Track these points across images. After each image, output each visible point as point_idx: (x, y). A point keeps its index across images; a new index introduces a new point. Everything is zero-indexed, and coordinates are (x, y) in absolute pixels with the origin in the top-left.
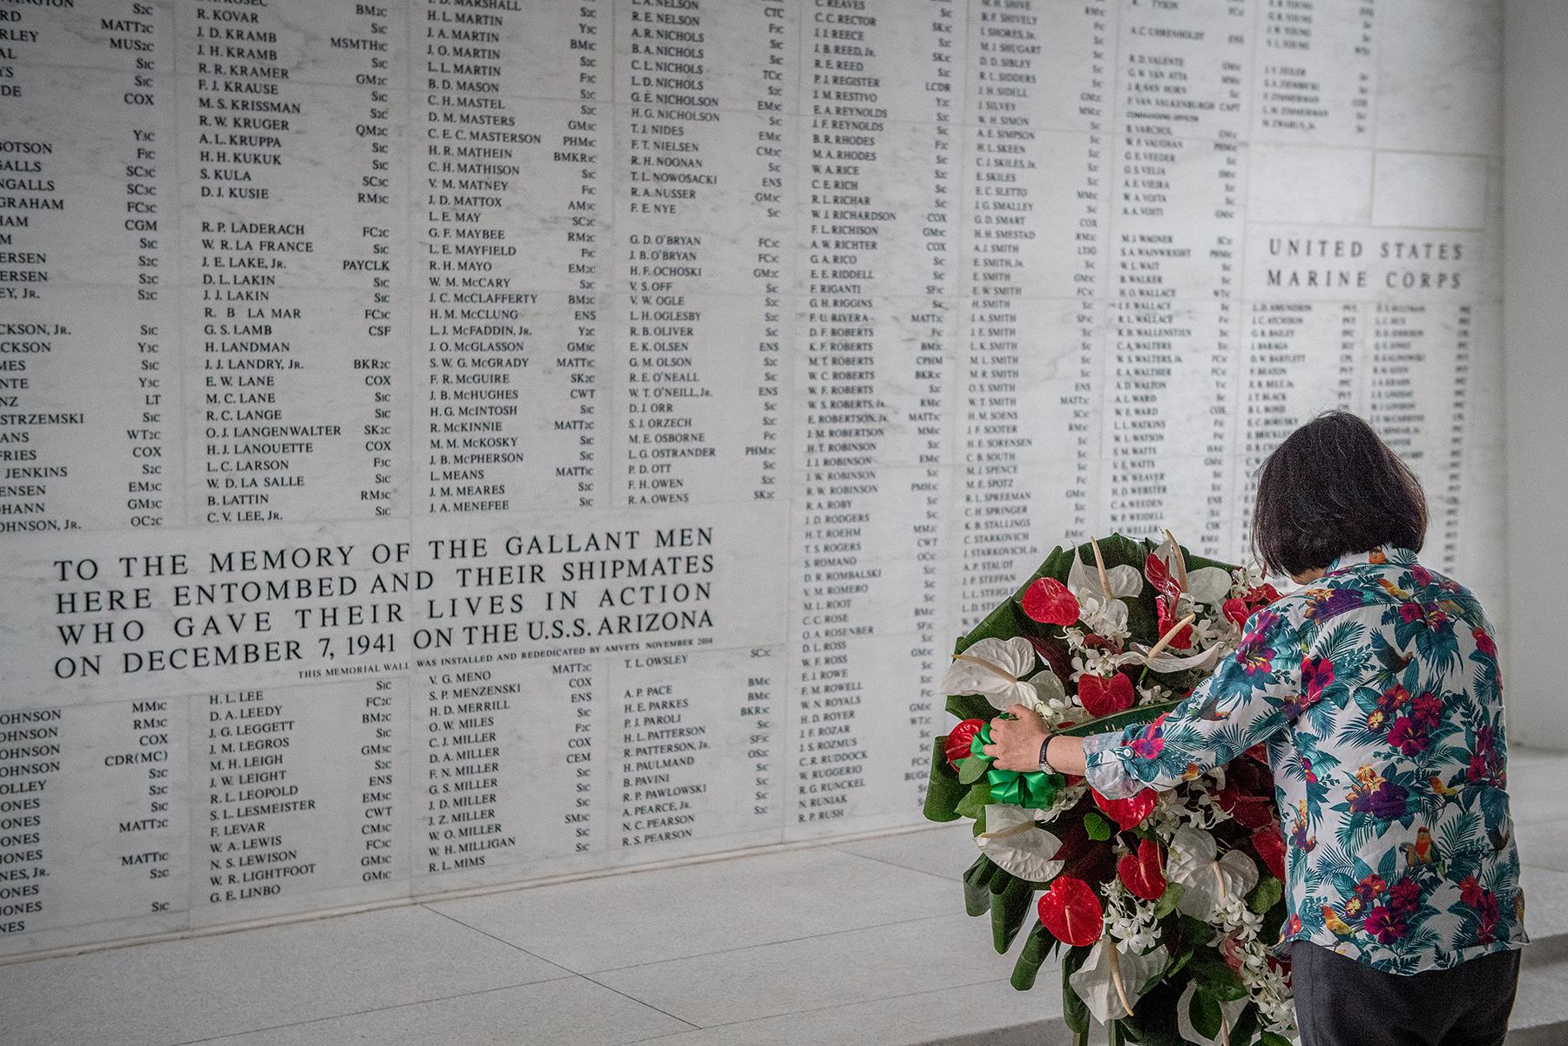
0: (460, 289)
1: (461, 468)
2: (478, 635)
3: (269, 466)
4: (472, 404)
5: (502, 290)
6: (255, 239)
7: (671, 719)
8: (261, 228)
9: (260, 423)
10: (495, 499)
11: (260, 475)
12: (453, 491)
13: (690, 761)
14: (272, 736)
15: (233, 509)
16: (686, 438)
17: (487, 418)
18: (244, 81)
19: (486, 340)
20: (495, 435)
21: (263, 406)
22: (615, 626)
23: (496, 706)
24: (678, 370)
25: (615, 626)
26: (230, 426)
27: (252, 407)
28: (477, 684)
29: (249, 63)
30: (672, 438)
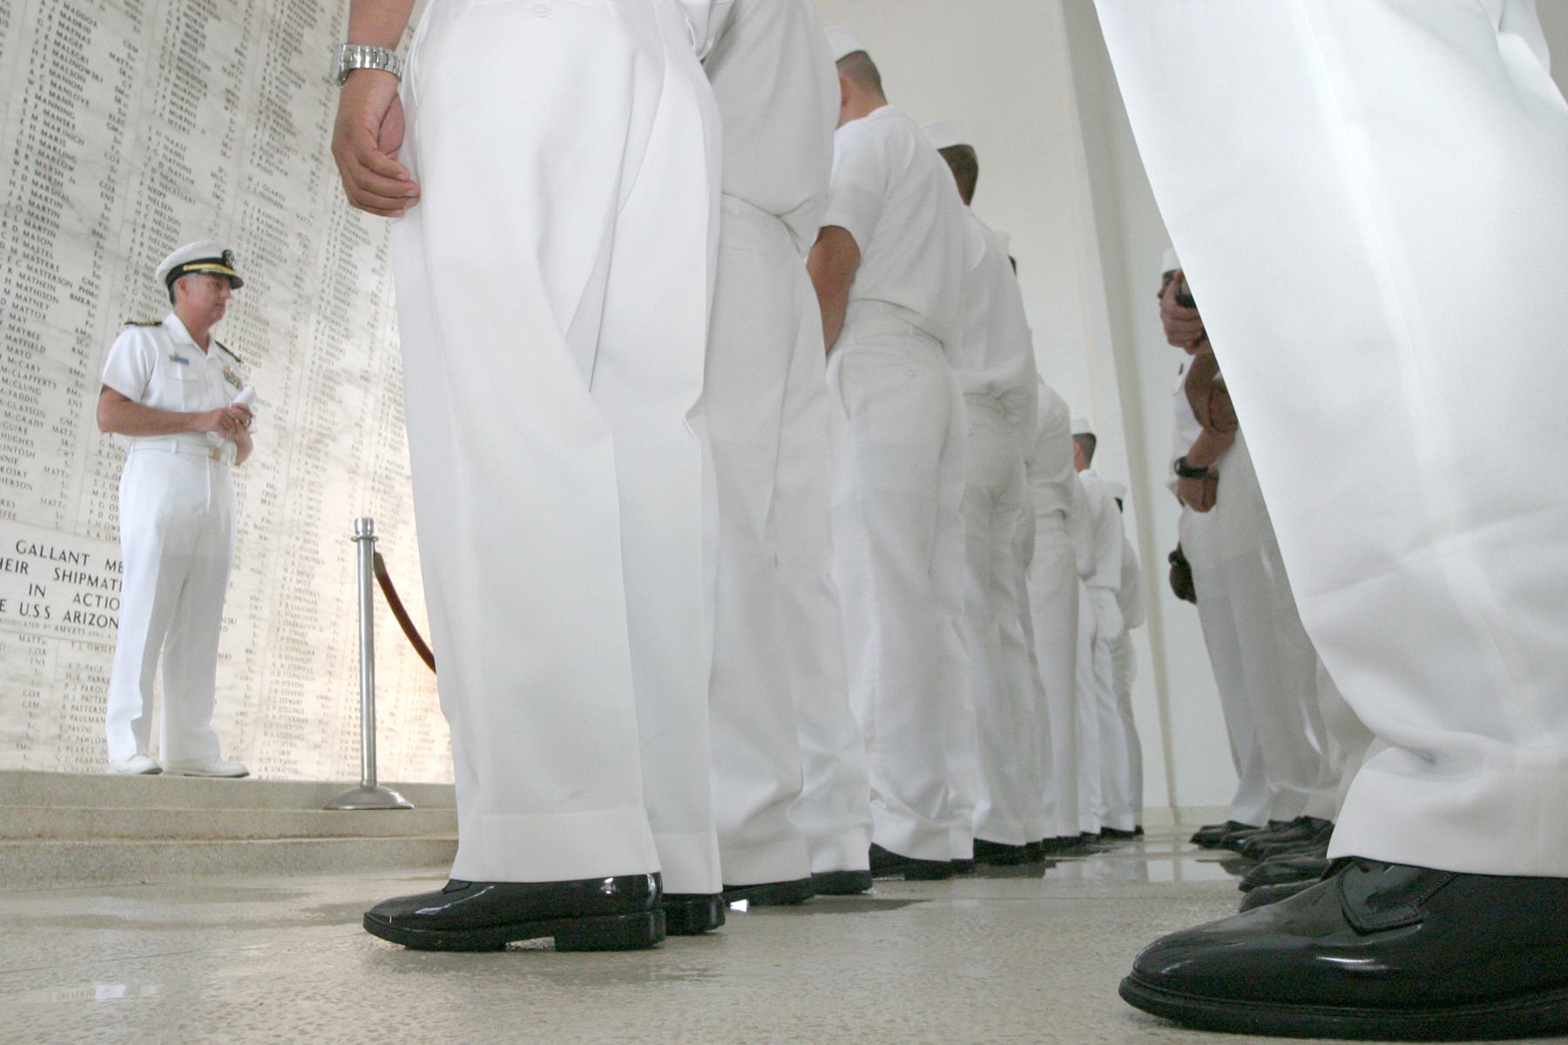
5: (35, 373)
19: (19, 403)
20: (13, 466)
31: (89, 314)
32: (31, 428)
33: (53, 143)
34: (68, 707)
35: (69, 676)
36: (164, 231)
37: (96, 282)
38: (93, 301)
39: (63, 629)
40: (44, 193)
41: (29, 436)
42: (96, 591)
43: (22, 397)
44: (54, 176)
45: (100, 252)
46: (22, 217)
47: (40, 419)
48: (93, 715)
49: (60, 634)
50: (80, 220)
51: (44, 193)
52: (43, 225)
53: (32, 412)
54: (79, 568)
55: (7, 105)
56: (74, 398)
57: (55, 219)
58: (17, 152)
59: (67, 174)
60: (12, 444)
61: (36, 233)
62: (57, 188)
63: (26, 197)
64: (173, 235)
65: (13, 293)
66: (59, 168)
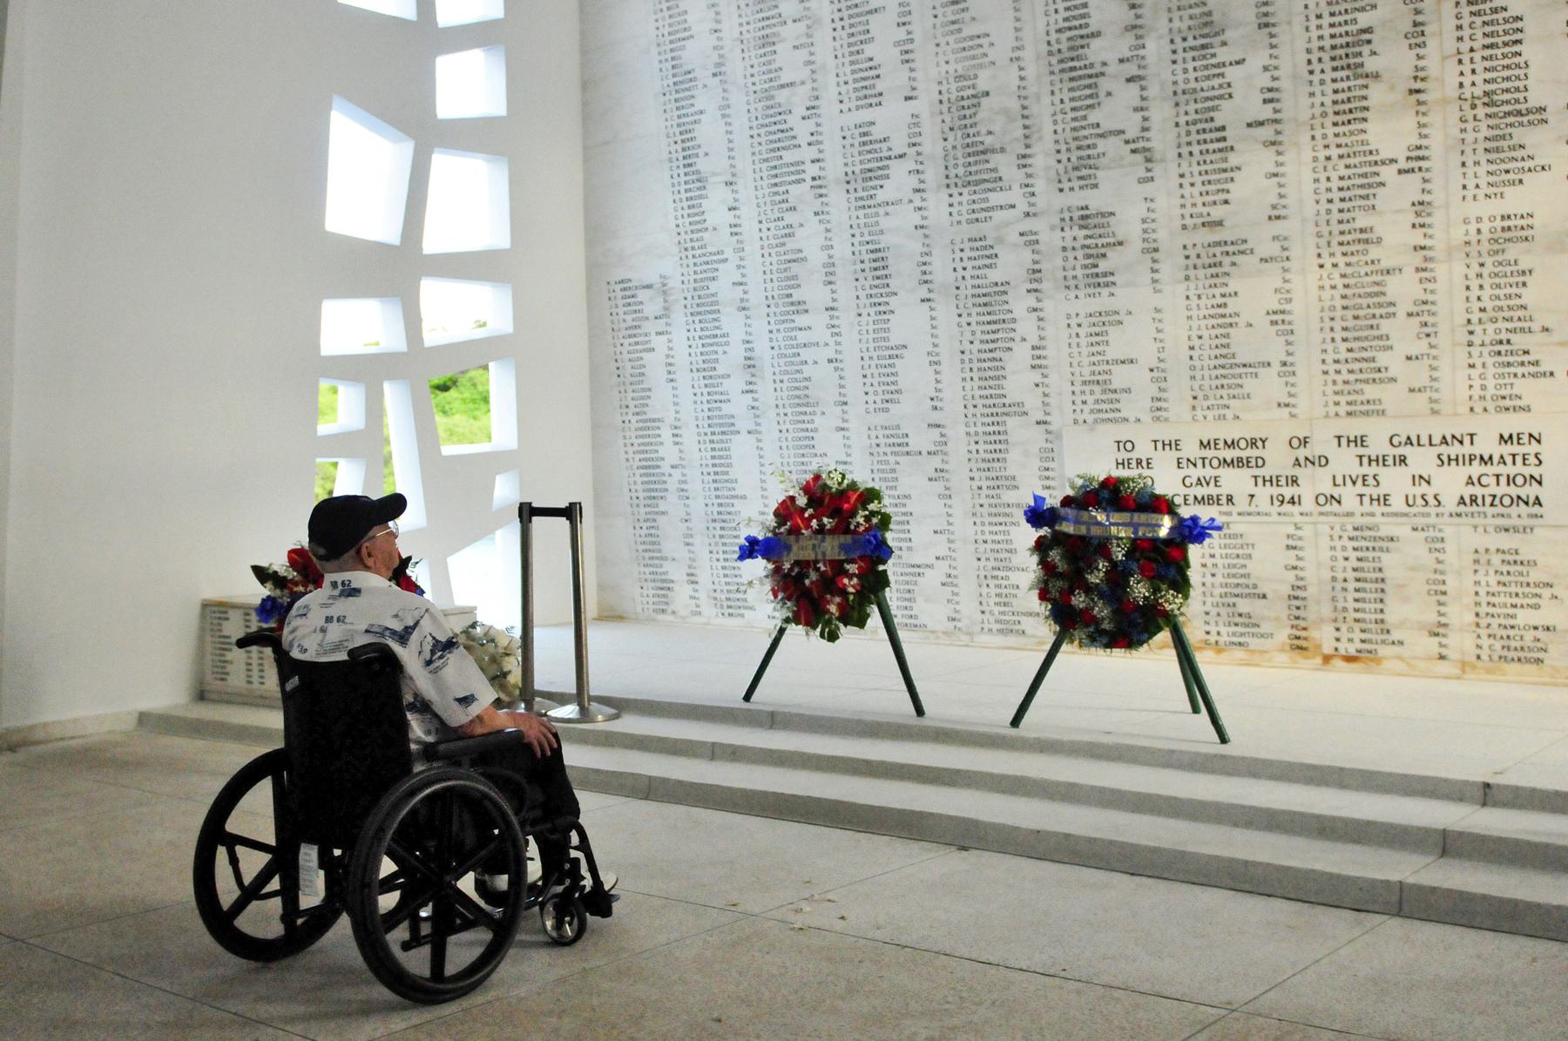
0: (1342, 268)
1: (1347, 388)
2: (1366, 500)
3: (1230, 387)
4: (1355, 345)
6: (1218, 250)
7: (1521, 574)
8: (1218, 244)
9: (1222, 361)
10: (1374, 410)
11: (1224, 392)
12: (1343, 403)
13: (1537, 607)
14: (1240, 552)
15: (1210, 414)
16: (1523, 364)
17: (1365, 355)
18: (1208, 158)
19: (1364, 302)
21: (1224, 351)
22: (1468, 501)
23: (1381, 549)
24: (1516, 314)
25: (1468, 501)
26: (1207, 362)
27: (1218, 352)
28: (1367, 533)
29: (1211, 147)
30: (1509, 364)
31: (1425, 181)
32: (1383, 322)
33: (1342, 30)
34: (1482, 592)
35: (1476, 561)
36: (1499, 40)
37: (1424, 142)
38: (1424, 164)
39: (1459, 515)
40: (1345, 85)
41: (1383, 331)
42: (1489, 469)
43: (1370, 295)
44: (1352, 61)
45: (1422, 109)
46: (1328, 122)
47: (1391, 310)
48: (1515, 601)
49: (1457, 520)
50: (1392, 88)
51: (1345, 85)
52: (1351, 116)
53: (1380, 305)
54: (1467, 449)
55: (1289, 23)
56: (1424, 275)
57: (1364, 103)
58: (1309, 62)
59: (1366, 50)
60: (1365, 344)
61: (1346, 129)
62: (1359, 71)
63: (1328, 101)
64: (1518, 36)
65: (1336, 200)
66: (1357, 49)
